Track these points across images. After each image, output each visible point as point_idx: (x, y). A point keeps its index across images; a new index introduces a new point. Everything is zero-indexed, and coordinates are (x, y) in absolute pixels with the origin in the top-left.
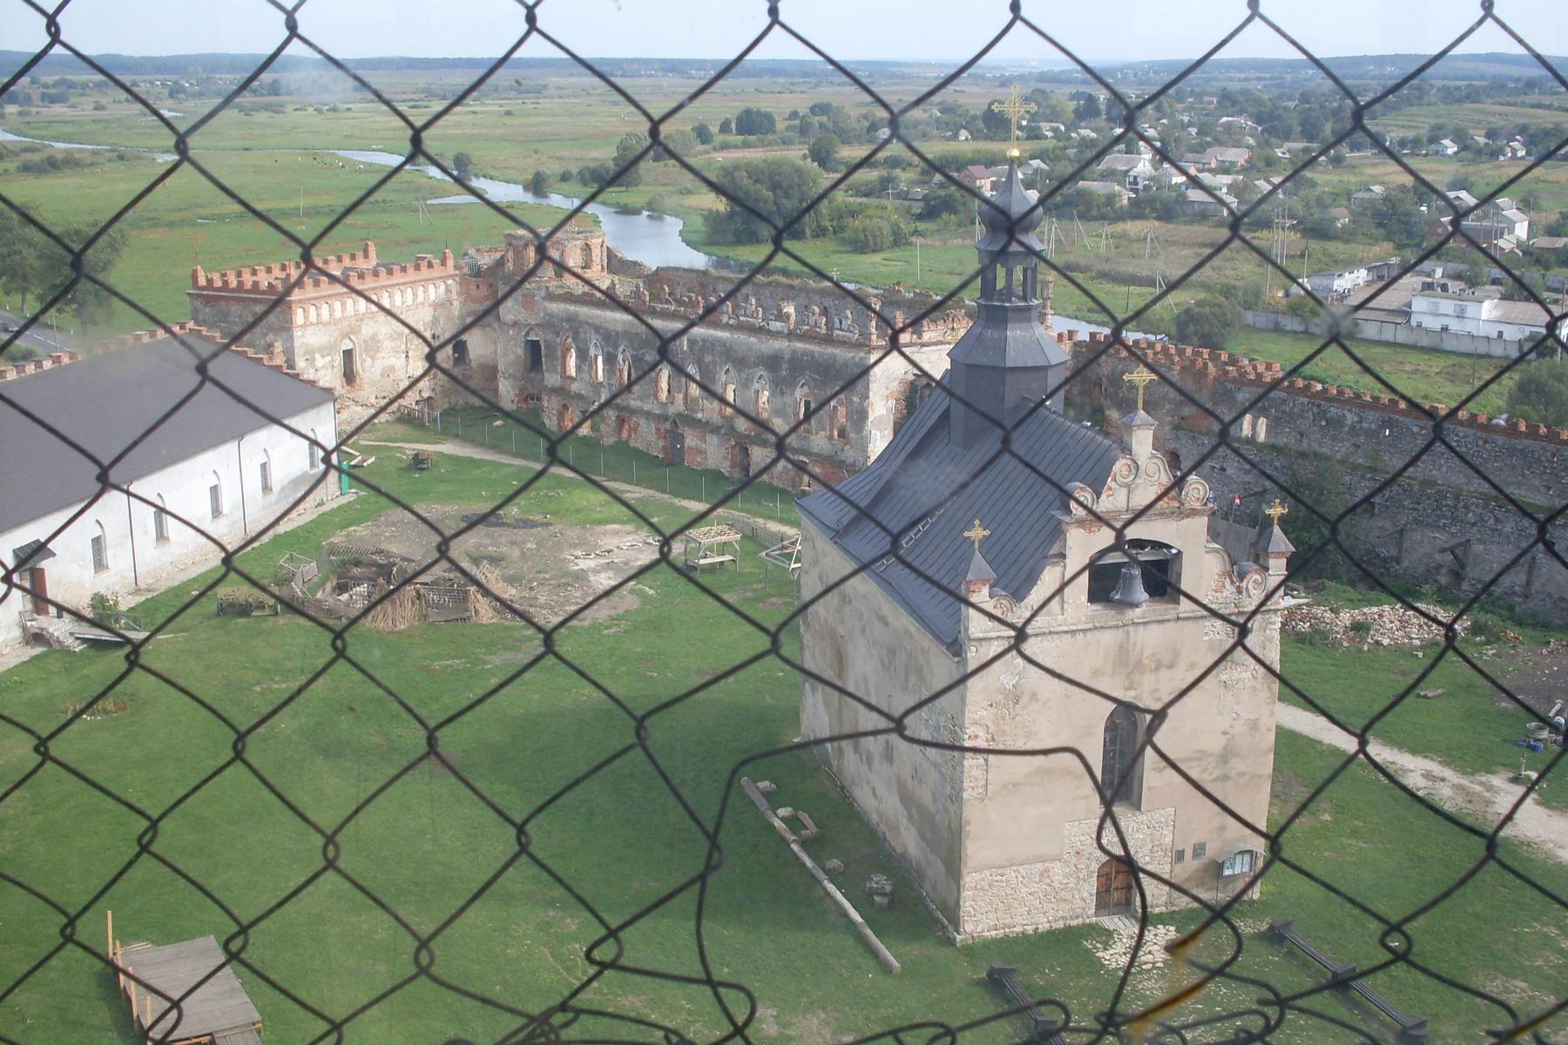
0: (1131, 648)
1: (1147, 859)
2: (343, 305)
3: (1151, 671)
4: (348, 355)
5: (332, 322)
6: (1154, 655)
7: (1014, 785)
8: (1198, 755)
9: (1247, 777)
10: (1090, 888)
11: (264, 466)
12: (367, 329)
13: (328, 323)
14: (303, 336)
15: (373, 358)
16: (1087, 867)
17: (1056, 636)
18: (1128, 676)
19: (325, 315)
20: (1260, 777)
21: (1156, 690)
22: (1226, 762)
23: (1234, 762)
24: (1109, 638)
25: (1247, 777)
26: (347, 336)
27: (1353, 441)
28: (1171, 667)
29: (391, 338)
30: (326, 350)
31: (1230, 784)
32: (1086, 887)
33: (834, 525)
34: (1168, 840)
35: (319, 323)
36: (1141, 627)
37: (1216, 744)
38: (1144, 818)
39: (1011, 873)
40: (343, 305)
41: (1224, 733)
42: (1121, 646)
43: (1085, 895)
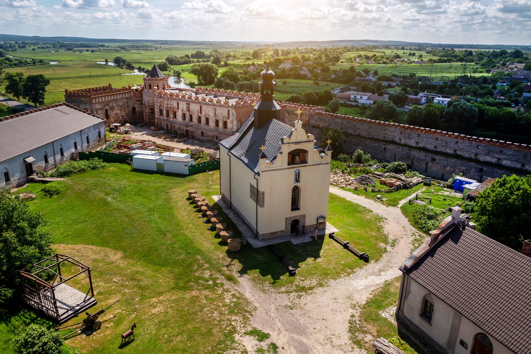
2: (105, 98)
4: (106, 110)
10: (289, 227)
11: (87, 137)
12: (111, 104)
15: (113, 111)
19: (100, 100)
26: (105, 106)
27: (342, 127)
32: (288, 226)
33: (228, 148)
40: (105, 98)
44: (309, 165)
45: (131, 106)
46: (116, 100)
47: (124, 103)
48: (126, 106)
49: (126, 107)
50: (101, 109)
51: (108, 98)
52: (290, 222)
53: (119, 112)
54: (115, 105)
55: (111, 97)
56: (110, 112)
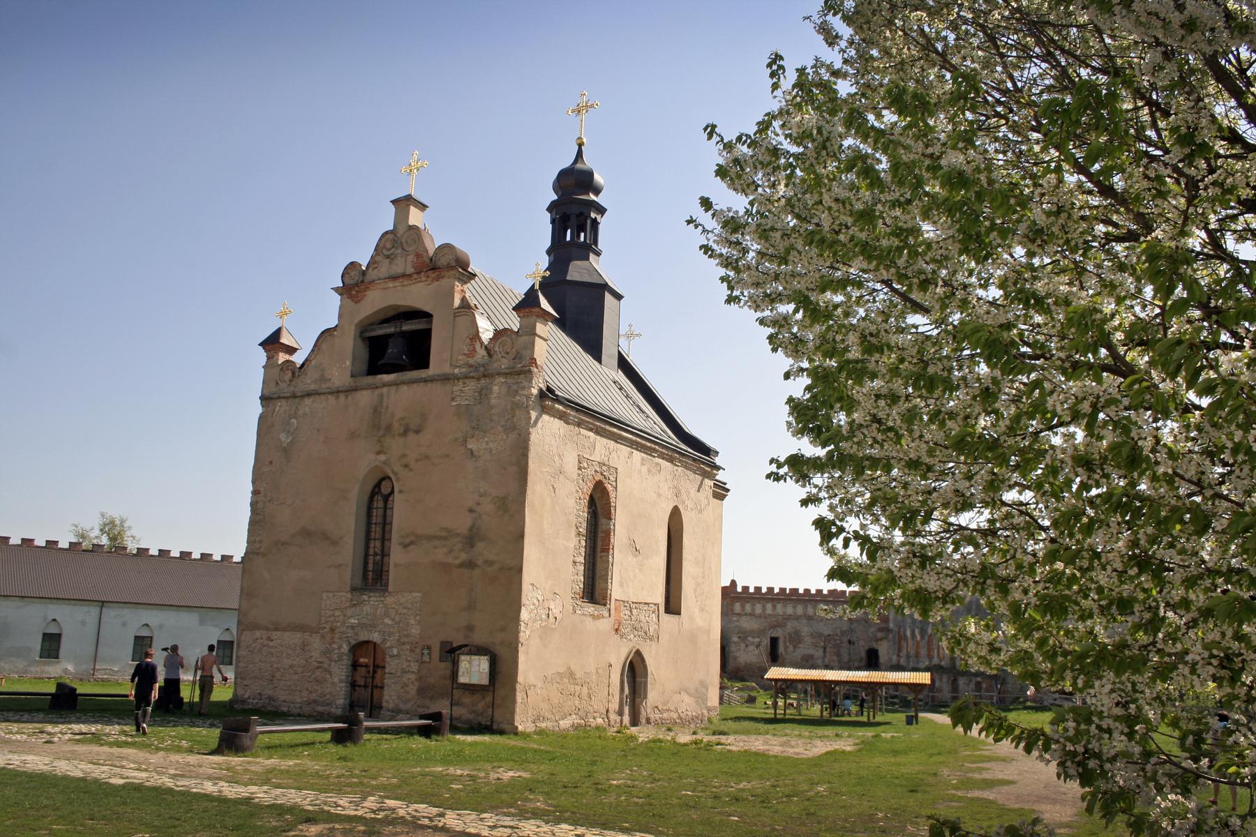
0: (383, 410)
1: (395, 651)
2: (774, 607)
3: (400, 435)
4: (774, 641)
5: (763, 616)
6: (403, 419)
7: (284, 544)
8: (444, 534)
9: (496, 567)
12: (790, 626)
13: (760, 616)
14: (738, 621)
15: (795, 647)
16: (339, 648)
17: (323, 397)
18: (379, 441)
20: (510, 569)
21: (404, 456)
22: (472, 546)
23: (480, 546)
24: (365, 398)
25: (496, 567)
26: (773, 627)
28: (417, 432)
29: (812, 635)
30: (752, 633)
31: (477, 572)
34: (415, 631)
35: (750, 615)
36: (394, 387)
37: (462, 524)
38: (390, 600)
39: (275, 635)
40: (774, 607)
41: (471, 511)
42: (376, 411)
43: (336, 680)
44: (431, 380)
45: (862, 643)
46: (810, 618)
47: (838, 632)
48: (845, 639)
49: (846, 644)
50: (761, 633)
51: (785, 606)
52: (345, 648)
53: (819, 653)
54: (805, 630)
55: (795, 607)
56: (786, 648)
